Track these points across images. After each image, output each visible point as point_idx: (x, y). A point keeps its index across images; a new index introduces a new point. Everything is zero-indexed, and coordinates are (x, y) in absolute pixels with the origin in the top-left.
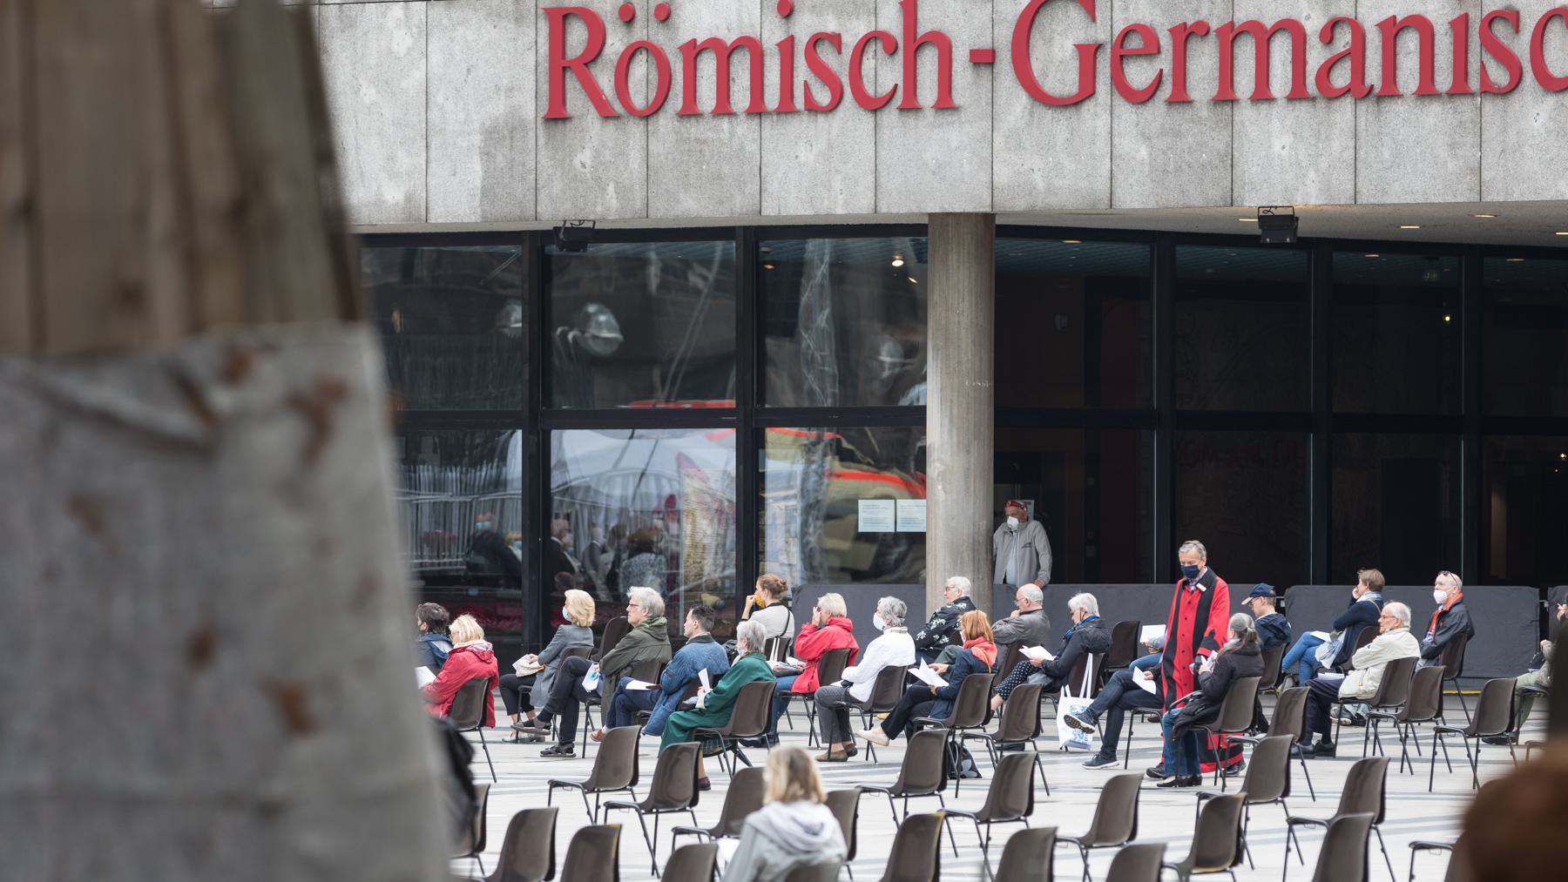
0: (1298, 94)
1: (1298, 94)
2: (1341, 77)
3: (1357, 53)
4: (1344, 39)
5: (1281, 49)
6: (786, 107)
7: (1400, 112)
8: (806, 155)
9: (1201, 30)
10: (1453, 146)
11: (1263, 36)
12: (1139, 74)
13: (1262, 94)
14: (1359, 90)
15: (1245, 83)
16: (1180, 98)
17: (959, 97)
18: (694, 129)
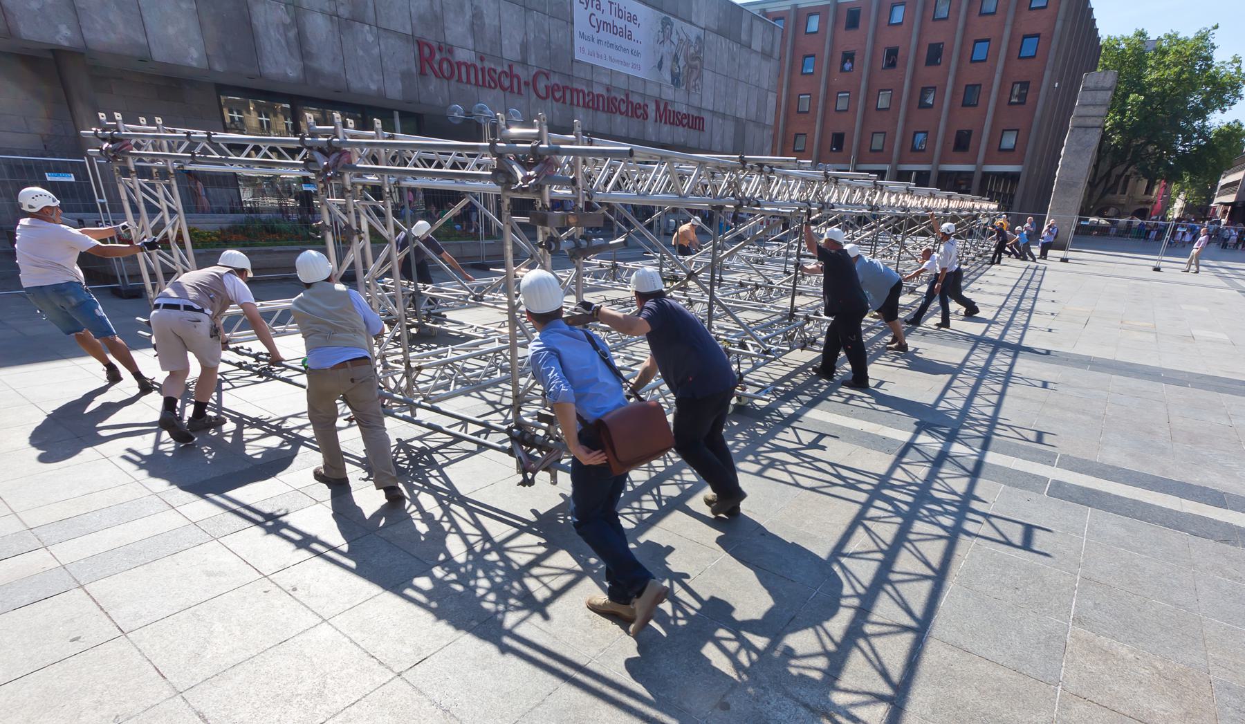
0: (584, 106)
1: (584, 106)
7: (599, 113)
12: (558, 95)
13: (578, 104)
16: (564, 102)
18: (461, 86)
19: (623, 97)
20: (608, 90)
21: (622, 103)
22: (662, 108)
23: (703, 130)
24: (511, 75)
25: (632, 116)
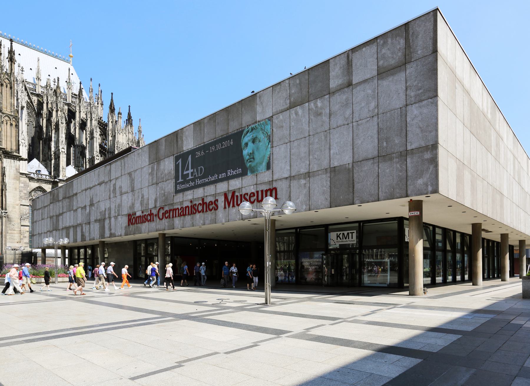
0: (178, 216)
1: (178, 216)
2: (182, 214)
5: (177, 211)
7: (186, 216)
9: (171, 210)
10: (191, 220)
11: (176, 209)
13: (176, 216)
14: (183, 215)
17: (154, 220)
18: (137, 225)
19: (201, 202)
20: (191, 202)
21: (199, 206)
22: (229, 197)
24: (151, 214)
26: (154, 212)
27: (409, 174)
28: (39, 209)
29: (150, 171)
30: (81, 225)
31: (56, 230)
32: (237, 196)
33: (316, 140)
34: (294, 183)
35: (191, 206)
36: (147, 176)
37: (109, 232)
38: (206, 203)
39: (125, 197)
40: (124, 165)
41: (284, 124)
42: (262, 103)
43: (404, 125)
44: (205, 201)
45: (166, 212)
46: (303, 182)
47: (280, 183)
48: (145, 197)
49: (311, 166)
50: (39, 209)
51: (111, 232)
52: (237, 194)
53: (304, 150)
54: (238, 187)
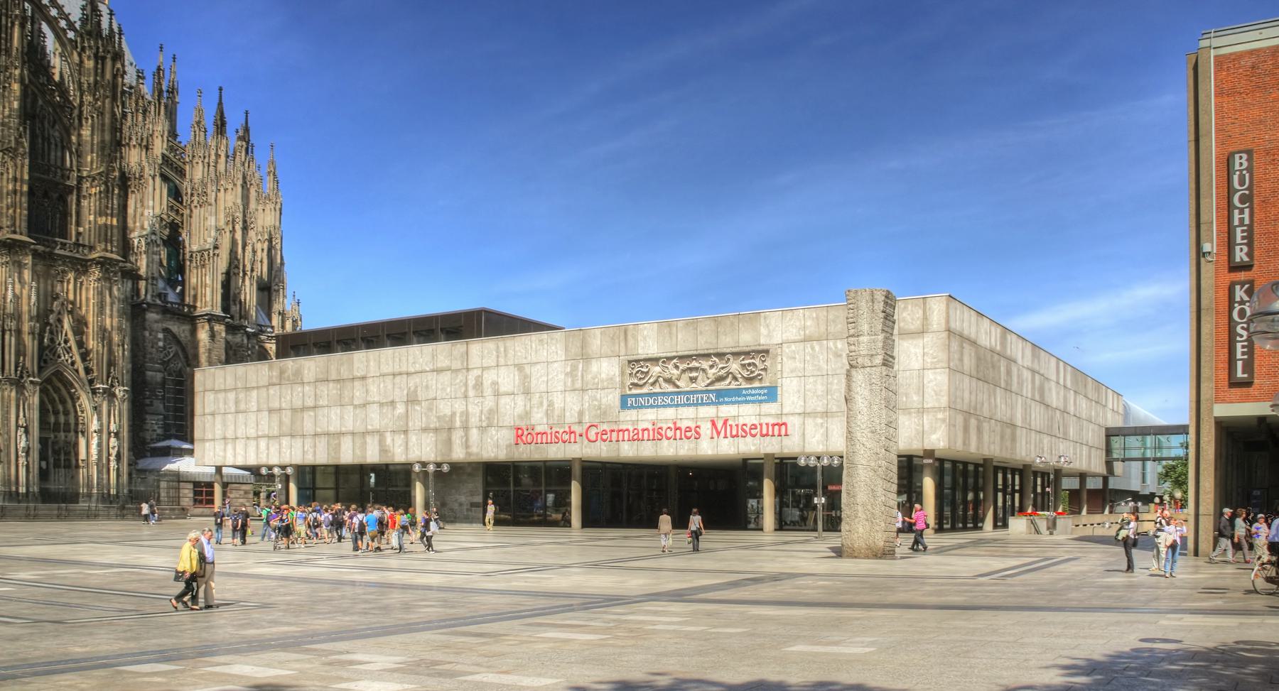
1: (629, 440)
3: (638, 434)
4: (636, 431)
6: (551, 443)
8: (554, 449)
11: (623, 431)
12: (605, 437)
15: (621, 438)
19: (672, 426)
23: (786, 435)
25: (681, 439)
26: (576, 428)
27: (926, 429)
28: (225, 390)
29: (568, 369)
30: (380, 433)
31: (292, 436)
32: (731, 426)
33: (836, 381)
34: (809, 421)
35: (654, 430)
36: (562, 377)
37: (464, 451)
38: (679, 429)
39: (504, 400)
40: (505, 351)
41: (797, 356)
42: (768, 326)
43: (921, 385)
44: (678, 425)
45: (604, 432)
46: (819, 421)
47: (791, 418)
48: (556, 406)
49: (829, 406)
50: (220, 391)
51: (470, 451)
52: (730, 422)
53: (820, 388)
54: (733, 415)
